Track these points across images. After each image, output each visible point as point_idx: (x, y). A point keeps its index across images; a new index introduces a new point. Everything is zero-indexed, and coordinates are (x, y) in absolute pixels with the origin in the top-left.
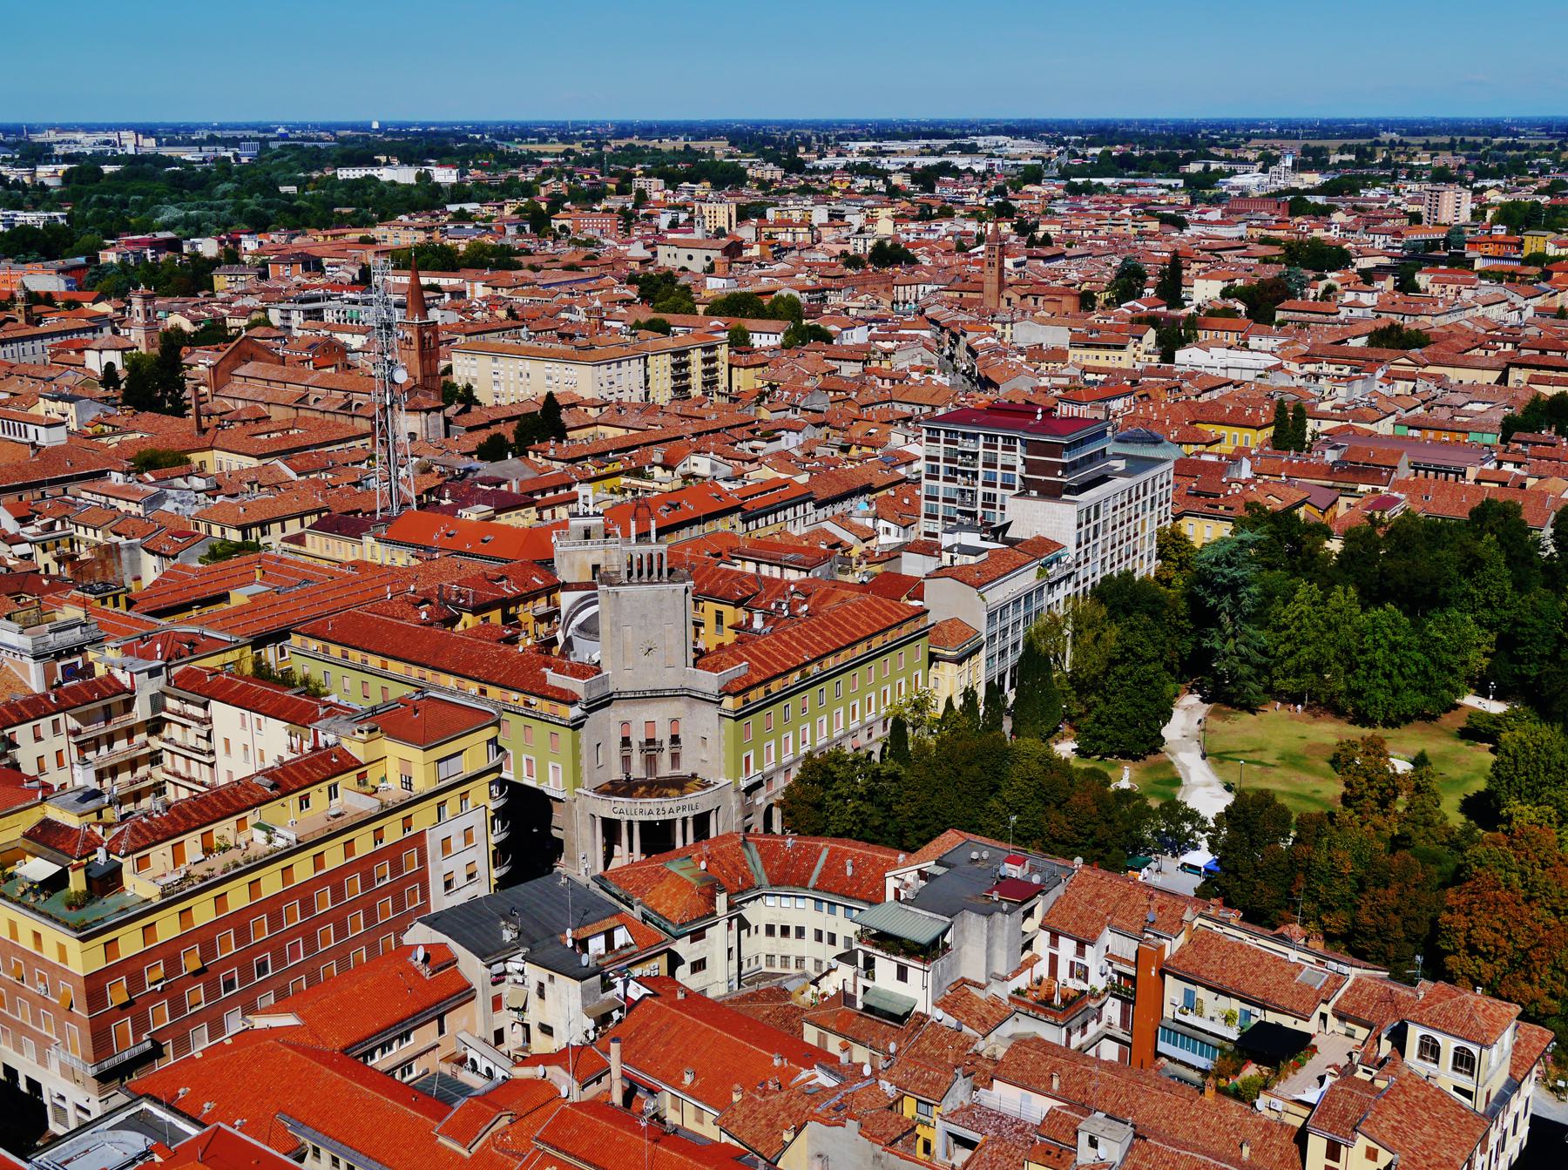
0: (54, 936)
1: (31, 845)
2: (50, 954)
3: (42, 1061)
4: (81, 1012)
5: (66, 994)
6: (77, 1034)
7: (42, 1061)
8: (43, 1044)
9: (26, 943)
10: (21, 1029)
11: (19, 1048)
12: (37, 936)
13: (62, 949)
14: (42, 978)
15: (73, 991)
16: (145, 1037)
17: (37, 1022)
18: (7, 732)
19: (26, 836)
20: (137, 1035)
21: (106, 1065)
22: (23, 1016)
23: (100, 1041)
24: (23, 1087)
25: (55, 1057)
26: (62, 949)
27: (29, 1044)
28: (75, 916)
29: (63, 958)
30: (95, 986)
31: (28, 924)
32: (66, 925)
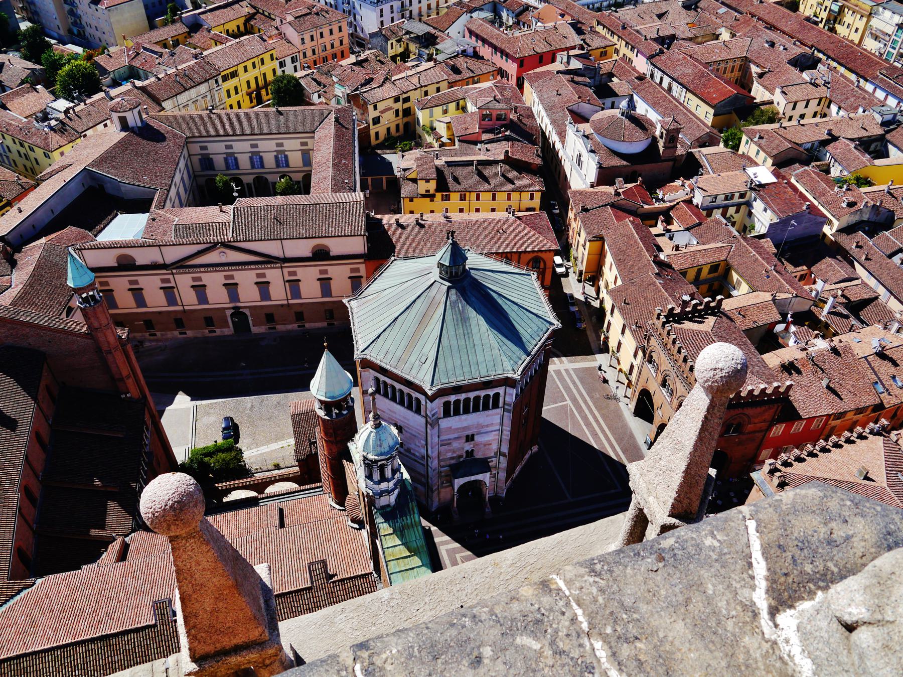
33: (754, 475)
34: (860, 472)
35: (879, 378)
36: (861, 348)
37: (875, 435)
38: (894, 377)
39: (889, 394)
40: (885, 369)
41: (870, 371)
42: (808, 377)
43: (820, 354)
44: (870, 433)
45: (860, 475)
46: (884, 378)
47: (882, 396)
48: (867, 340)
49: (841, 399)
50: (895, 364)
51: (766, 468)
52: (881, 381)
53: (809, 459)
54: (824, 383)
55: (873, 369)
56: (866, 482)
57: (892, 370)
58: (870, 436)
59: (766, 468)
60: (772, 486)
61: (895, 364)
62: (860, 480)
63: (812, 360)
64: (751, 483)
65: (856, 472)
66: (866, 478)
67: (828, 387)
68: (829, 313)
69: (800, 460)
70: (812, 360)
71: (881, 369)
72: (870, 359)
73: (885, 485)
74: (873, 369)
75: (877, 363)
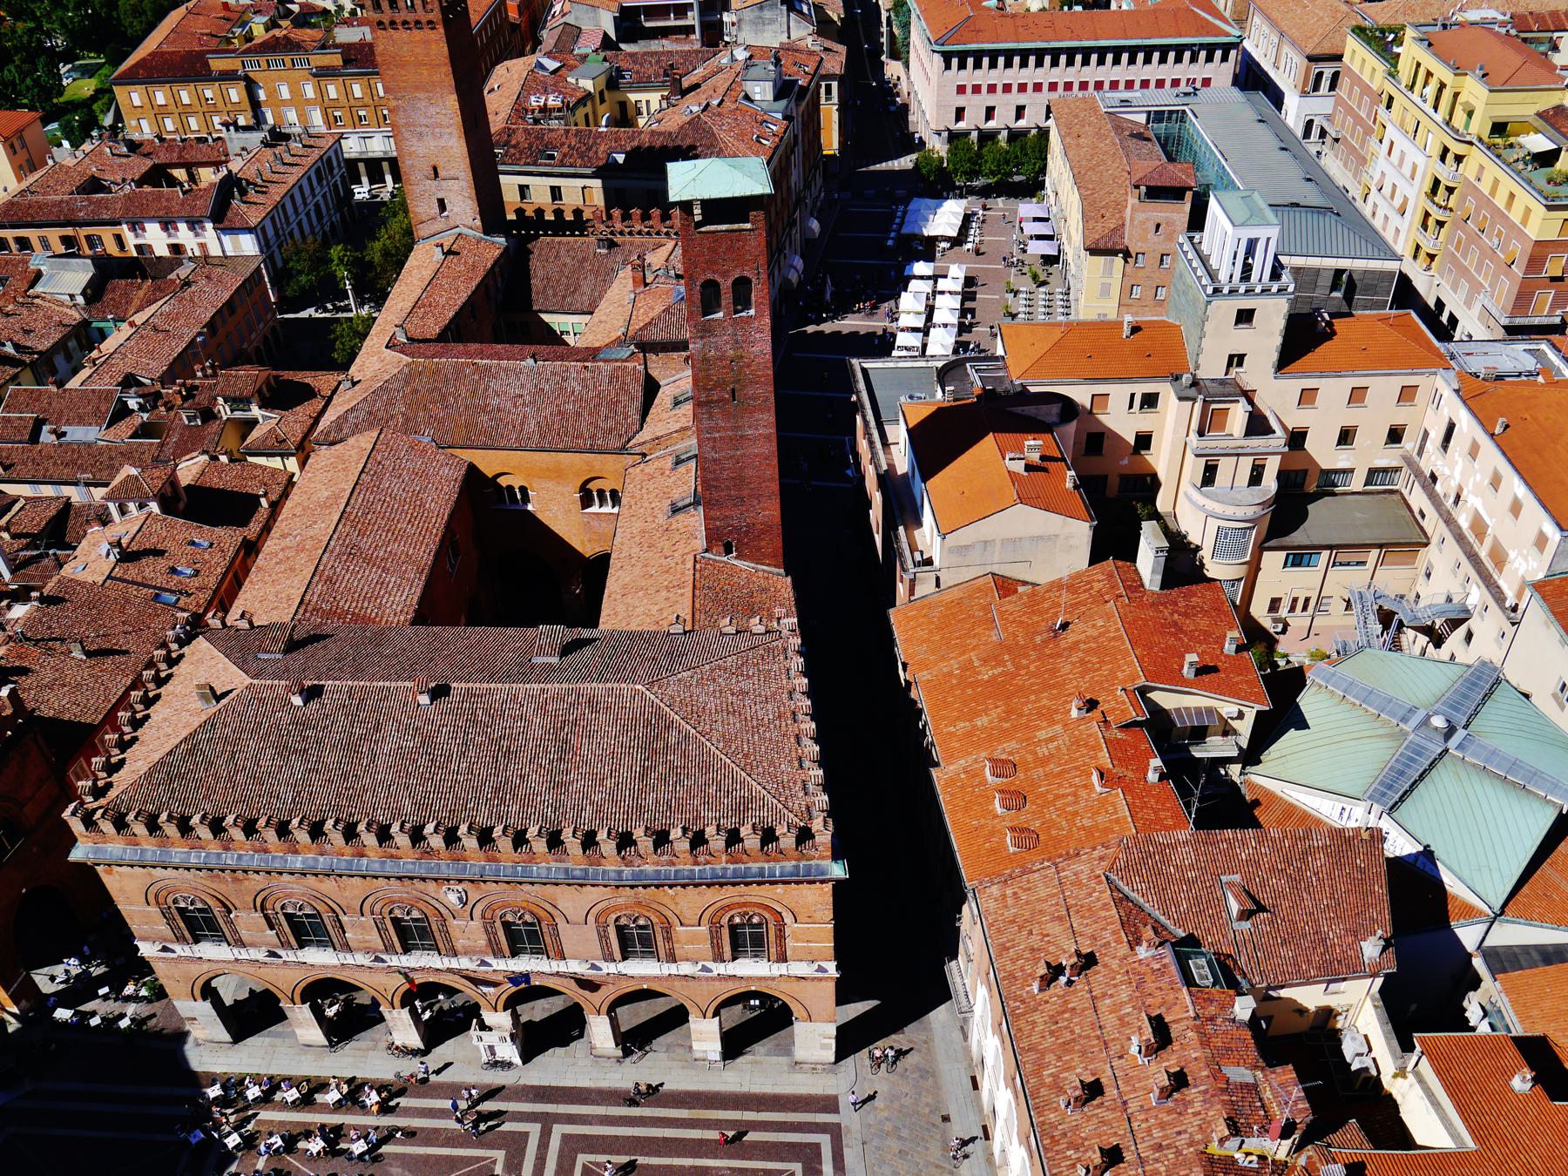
0: (1525, 199)
1: (1539, 123)
2: (1515, 216)
3: (1468, 303)
4: (1518, 271)
5: (1514, 252)
6: (1507, 288)
7: (1468, 303)
8: (1476, 288)
9: (1500, 201)
10: (1464, 272)
11: (1455, 288)
12: (1512, 196)
13: (1528, 211)
14: (1499, 235)
15: (1520, 251)
16: (1558, 312)
17: (1478, 271)
18: (1556, 35)
19: (1539, 115)
20: (1553, 307)
21: (1518, 321)
22: (1470, 262)
23: (1523, 299)
24: (1444, 318)
25: (1482, 299)
26: (1528, 211)
27: (1465, 285)
28: (1550, 189)
29: (1525, 222)
30: (1540, 252)
31: (1508, 184)
32: (1540, 192)
33: (76, 855)
34: (203, 697)
35: (155, 587)
36: (94, 572)
37: (189, 643)
38: (173, 570)
39: (189, 595)
40: (151, 570)
41: (133, 590)
42: (45, 668)
43: (30, 621)
44: (181, 647)
45: (208, 701)
46: (160, 581)
47: (181, 604)
48: (93, 556)
49: (126, 652)
50: (158, 553)
51: (77, 826)
52: (159, 588)
53: (128, 754)
54: (77, 654)
55: (133, 583)
56: (224, 701)
57: (162, 564)
58: (186, 650)
59: (77, 826)
60: (112, 841)
61: (158, 553)
62: (214, 707)
63: (28, 639)
64: (87, 872)
65: (200, 704)
66: (218, 698)
67: (89, 654)
68: (12, 572)
69: (112, 768)
70: (28, 639)
71: (146, 574)
72: (118, 572)
73: (249, 681)
74: (133, 583)
75: (132, 571)
